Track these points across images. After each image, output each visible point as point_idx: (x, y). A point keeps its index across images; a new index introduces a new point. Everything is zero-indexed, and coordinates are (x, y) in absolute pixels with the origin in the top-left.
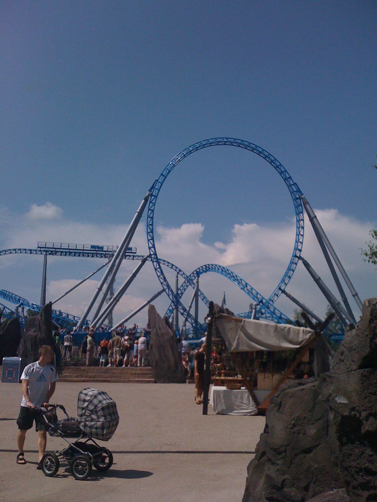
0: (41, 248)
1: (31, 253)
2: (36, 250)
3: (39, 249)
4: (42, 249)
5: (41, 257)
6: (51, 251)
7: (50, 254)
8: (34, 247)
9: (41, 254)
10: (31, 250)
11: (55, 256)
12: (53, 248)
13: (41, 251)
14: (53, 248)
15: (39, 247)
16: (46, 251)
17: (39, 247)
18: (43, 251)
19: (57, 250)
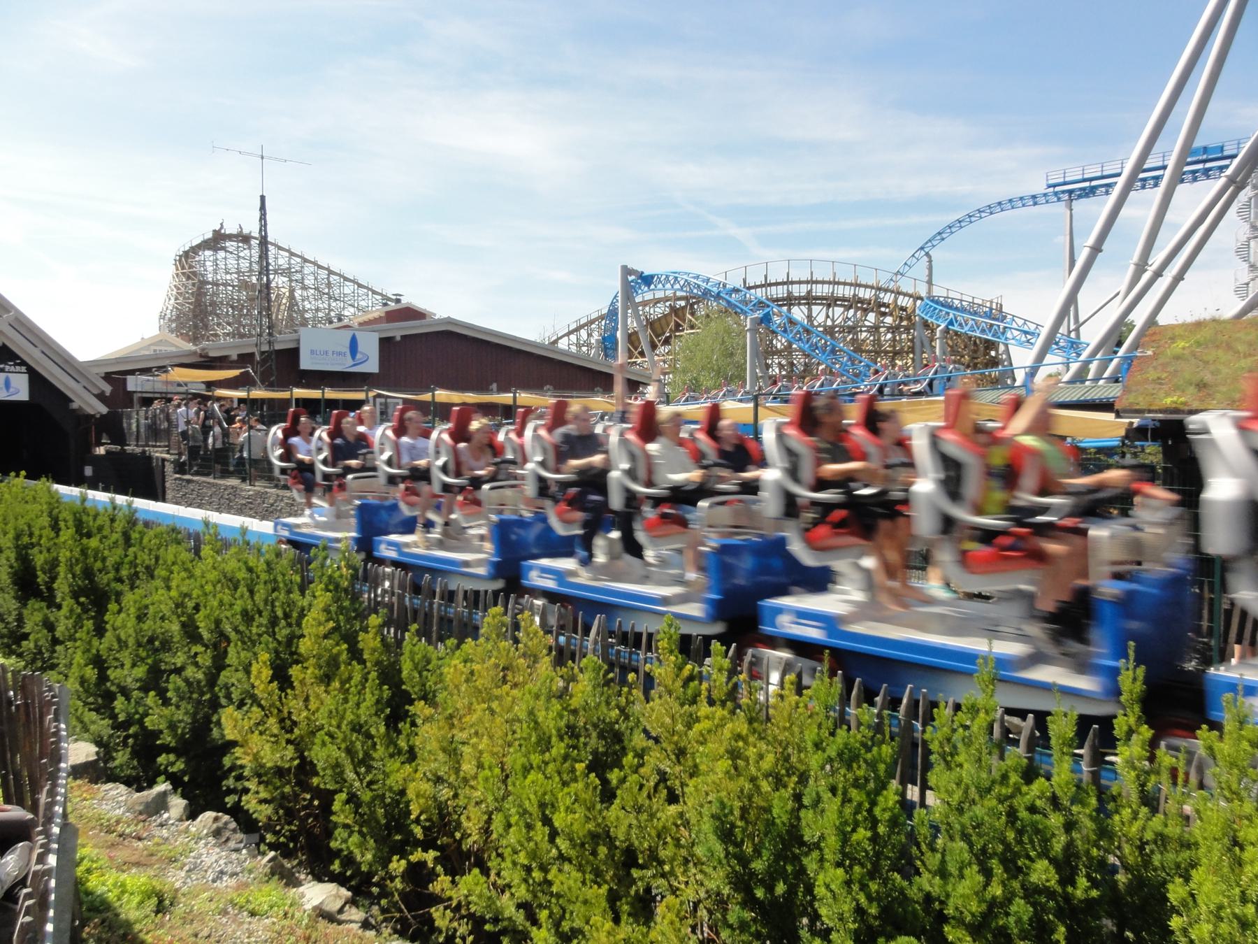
0: (1054, 186)
1: (1035, 204)
2: (1045, 195)
3: (1051, 189)
4: (1058, 189)
5: (1060, 209)
6: (1081, 189)
7: (1080, 197)
8: (1040, 188)
9: (1059, 199)
10: (1034, 197)
11: (1092, 199)
12: (1084, 180)
13: (1056, 194)
14: (1084, 180)
15: (1049, 186)
16: (1071, 192)
17: (1049, 186)
18: (1063, 192)
19: (1094, 183)
